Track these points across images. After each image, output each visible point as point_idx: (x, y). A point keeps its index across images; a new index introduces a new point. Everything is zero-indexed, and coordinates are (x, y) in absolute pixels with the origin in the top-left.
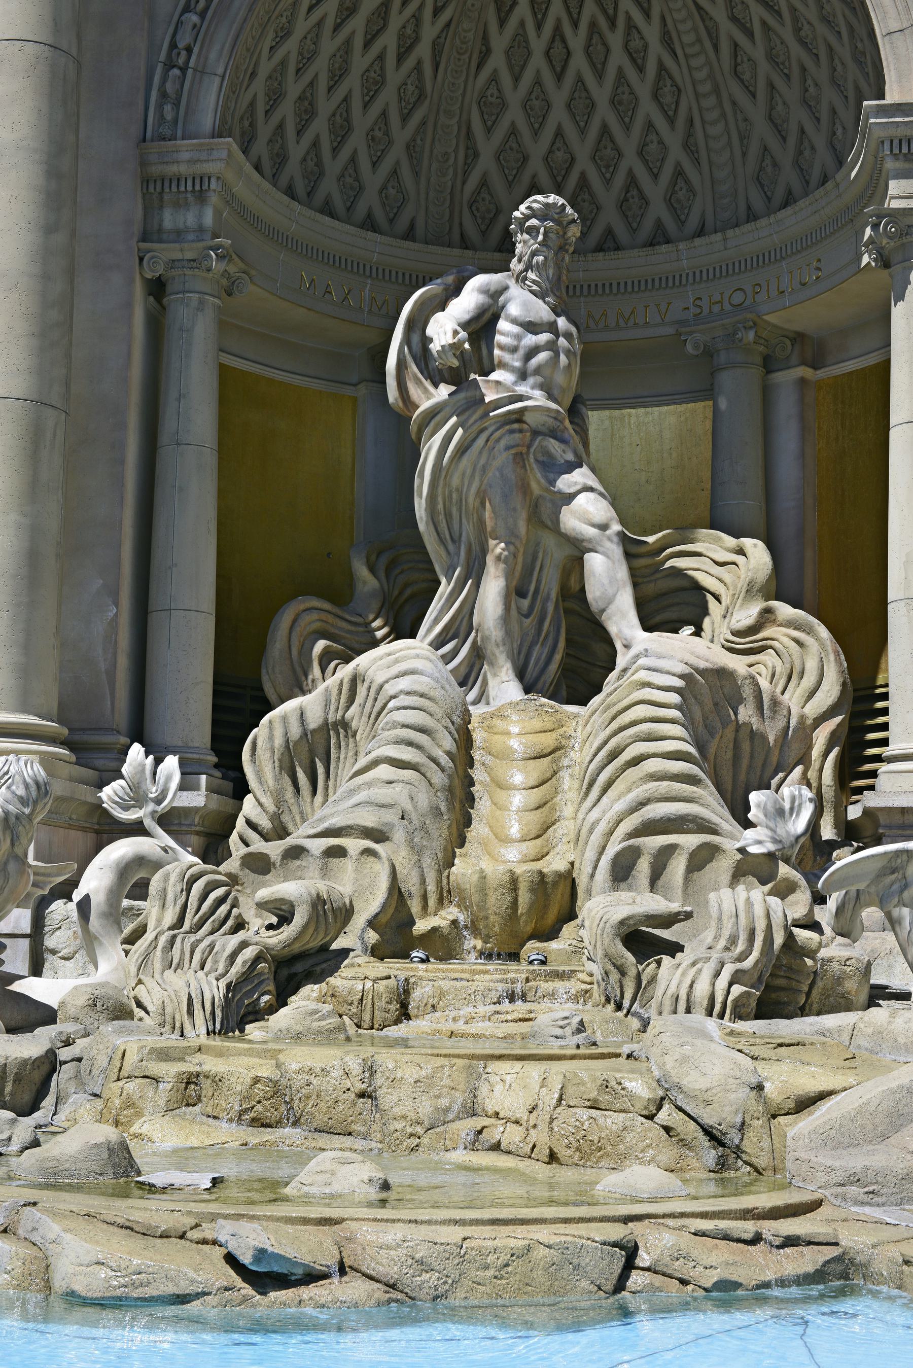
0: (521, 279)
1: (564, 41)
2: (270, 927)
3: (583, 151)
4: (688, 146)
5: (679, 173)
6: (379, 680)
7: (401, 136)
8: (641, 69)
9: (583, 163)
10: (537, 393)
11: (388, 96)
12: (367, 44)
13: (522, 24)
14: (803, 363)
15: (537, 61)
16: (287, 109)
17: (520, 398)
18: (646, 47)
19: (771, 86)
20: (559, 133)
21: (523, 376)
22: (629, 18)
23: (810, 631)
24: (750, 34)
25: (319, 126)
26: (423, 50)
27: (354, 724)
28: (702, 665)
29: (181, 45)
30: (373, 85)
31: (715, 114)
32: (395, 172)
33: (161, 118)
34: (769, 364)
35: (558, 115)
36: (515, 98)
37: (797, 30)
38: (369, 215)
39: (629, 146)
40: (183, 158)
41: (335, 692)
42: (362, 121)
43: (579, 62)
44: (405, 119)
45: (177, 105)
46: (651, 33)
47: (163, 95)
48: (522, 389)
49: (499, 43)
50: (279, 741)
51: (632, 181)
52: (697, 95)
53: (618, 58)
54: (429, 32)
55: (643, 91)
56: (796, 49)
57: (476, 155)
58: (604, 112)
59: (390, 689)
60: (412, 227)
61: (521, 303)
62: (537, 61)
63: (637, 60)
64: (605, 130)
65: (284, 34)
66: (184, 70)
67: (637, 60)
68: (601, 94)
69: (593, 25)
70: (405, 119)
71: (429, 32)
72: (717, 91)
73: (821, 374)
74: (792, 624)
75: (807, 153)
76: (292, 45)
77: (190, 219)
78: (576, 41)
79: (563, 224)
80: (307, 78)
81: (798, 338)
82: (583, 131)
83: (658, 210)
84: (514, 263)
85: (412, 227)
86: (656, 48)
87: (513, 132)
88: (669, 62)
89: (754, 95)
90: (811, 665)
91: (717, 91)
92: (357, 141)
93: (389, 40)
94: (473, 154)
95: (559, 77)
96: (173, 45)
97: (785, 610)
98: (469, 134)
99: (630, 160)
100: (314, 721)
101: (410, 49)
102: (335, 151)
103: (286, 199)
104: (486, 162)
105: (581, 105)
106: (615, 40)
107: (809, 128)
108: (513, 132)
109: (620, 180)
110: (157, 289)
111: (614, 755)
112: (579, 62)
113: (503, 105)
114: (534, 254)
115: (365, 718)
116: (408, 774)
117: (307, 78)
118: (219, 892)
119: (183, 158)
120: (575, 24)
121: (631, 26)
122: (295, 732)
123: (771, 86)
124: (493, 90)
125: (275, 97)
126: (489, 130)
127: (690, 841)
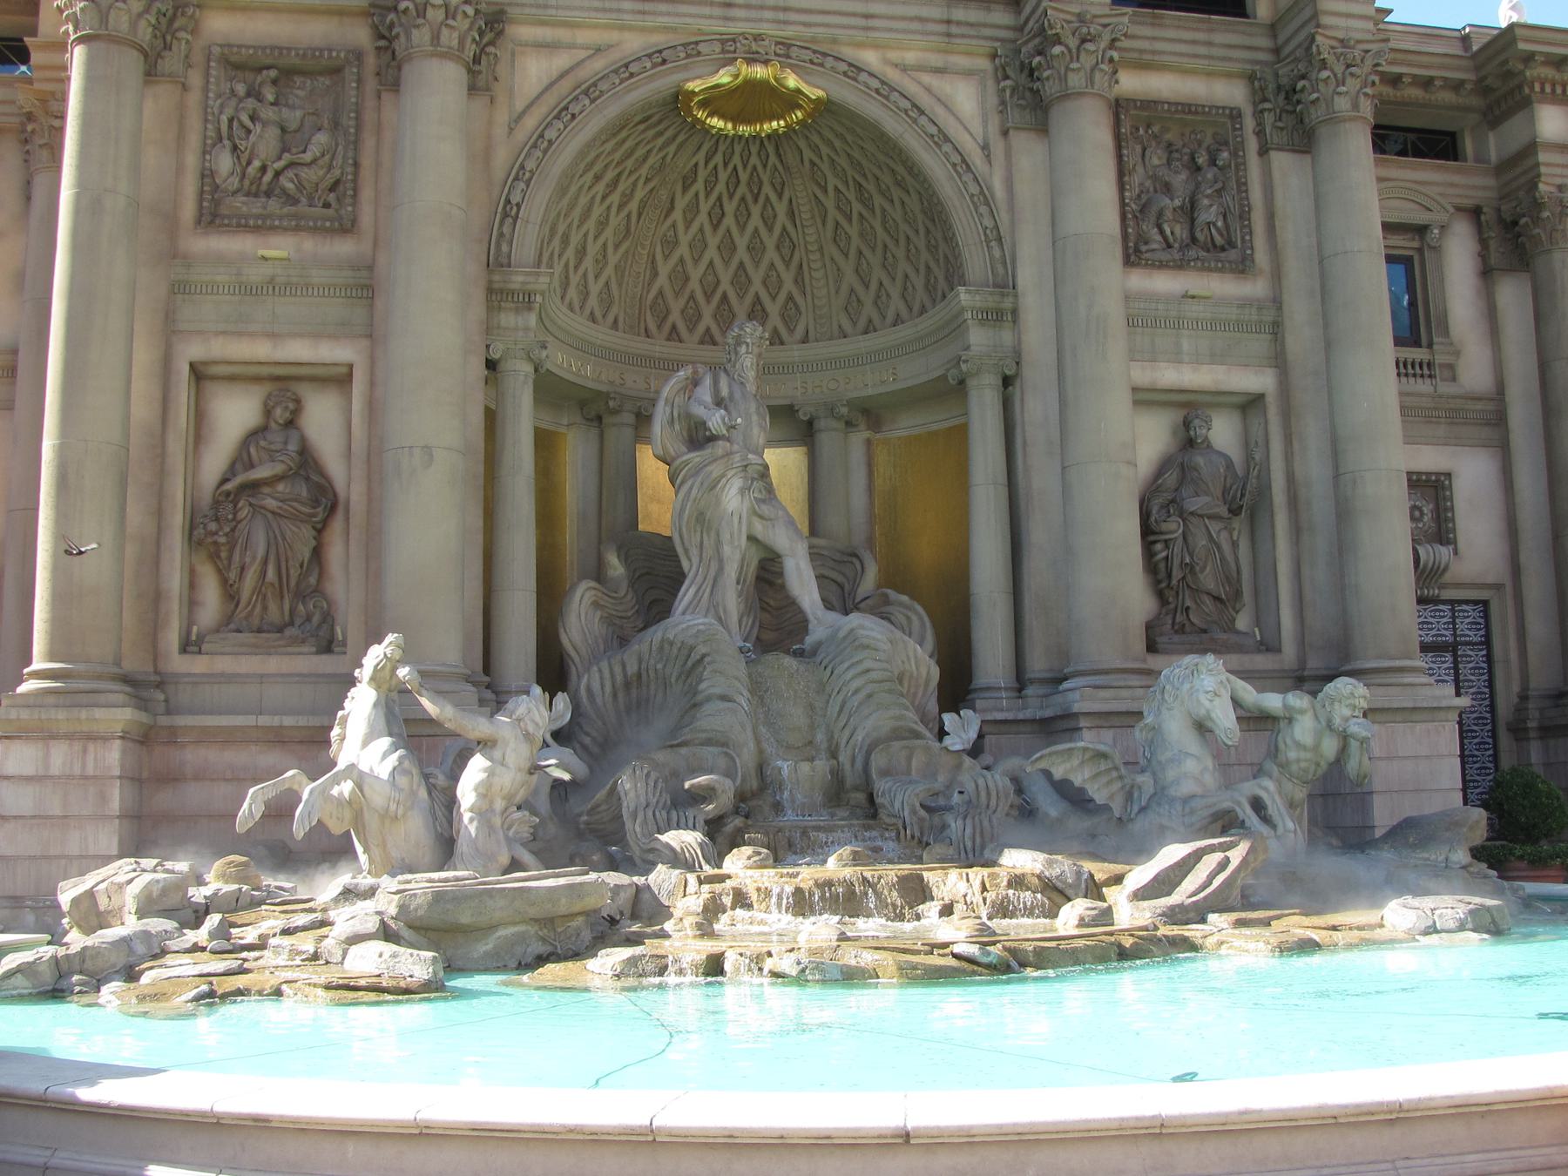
3: (725, 277)
4: (799, 281)
5: (790, 298)
7: (613, 259)
8: (770, 229)
9: (725, 286)
11: (608, 233)
15: (703, 218)
18: (775, 216)
20: (711, 263)
22: (767, 198)
26: (633, 206)
29: (514, 202)
30: (603, 224)
31: (819, 264)
35: (711, 253)
36: (684, 239)
37: (884, 222)
39: (757, 277)
40: (517, 281)
42: (593, 249)
47: (501, 235)
49: (681, 204)
53: (755, 221)
54: (640, 194)
55: (770, 243)
58: (742, 254)
60: (616, 321)
62: (703, 218)
64: (741, 265)
68: (741, 242)
69: (743, 199)
71: (640, 194)
72: (821, 249)
73: (878, 436)
74: (901, 604)
75: (884, 298)
78: (730, 208)
85: (616, 321)
86: (782, 217)
88: (790, 228)
91: (821, 249)
92: (588, 263)
94: (655, 274)
95: (715, 227)
96: (508, 201)
99: (757, 286)
101: (626, 204)
104: (662, 280)
106: (756, 210)
107: (886, 282)
108: (682, 260)
110: (491, 365)
112: (729, 221)
113: (676, 243)
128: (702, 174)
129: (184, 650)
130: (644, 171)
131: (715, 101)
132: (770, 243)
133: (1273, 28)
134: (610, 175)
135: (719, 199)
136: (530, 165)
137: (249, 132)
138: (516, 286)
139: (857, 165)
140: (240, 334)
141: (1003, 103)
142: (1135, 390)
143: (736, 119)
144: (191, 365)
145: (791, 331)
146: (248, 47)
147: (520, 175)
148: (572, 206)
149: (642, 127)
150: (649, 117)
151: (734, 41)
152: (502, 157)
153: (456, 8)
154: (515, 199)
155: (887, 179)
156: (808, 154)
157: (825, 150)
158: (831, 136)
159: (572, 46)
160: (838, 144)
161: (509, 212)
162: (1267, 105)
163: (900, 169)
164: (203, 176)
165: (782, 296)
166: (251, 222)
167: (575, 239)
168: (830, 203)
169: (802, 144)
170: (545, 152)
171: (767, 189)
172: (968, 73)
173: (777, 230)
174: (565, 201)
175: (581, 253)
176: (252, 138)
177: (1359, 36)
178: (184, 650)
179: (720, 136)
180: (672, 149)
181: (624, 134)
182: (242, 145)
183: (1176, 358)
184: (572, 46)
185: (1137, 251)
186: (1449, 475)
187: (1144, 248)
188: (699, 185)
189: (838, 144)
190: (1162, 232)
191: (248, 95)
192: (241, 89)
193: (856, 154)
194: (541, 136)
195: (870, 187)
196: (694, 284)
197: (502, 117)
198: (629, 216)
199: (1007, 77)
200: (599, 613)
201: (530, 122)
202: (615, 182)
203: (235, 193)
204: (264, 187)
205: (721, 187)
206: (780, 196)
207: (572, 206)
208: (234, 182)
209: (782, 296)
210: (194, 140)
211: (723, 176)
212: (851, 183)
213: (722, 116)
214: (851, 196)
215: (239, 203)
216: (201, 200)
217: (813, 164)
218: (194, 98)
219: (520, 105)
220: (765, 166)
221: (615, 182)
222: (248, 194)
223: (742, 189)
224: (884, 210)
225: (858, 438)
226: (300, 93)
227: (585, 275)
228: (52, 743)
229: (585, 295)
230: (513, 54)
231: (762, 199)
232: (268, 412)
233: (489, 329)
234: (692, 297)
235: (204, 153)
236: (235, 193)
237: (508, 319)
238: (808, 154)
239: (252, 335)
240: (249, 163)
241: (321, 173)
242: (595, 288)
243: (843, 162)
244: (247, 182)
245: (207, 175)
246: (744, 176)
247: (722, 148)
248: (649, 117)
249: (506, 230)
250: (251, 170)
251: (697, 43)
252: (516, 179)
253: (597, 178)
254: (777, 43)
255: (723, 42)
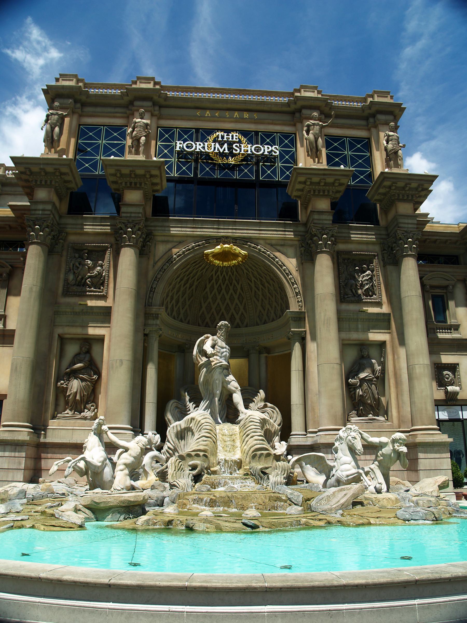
0: (219, 338)
1: (221, 287)
2: (190, 470)
4: (245, 308)
5: (242, 314)
6: (199, 419)
8: (236, 293)
9: (223, 310)
10: (224, 361)
12: (184, 285)
13: (213, 283)
14: (266, 353)
15: (215, 290)
17: (221, 362)
18: (237, 289)
19: (262, 300)
20: (218, 304)
21: (221, 357)
22: (234, 284)
23: (274, 409)
24: (259, 290)
25: (174, 301)
26: (194, 287)
27: (192, 428)
28: (262, 418)
29: (153, 287)
30: (184, 294)
32: (186, 310)
33: (149, 301)
34: (260, 353)
35: (218, 300)
37: (269, 291)
38: (181, 319)
40: (154, 310)
41: (187, 421)
42: (181, 300)
43: (224, 291)
44: (189, 300)
45: (152, 299)
46: (239, 287)
47: (149, 297)
48: (221, 360)
49: (208, 286)
50: (175, 431)
51: (233, 315)
52: (247, 299)
53: (231, 291)
54: (196, 283)
55: (236, 297)
56: (268, 294)
57: (202, 307)
58: (228, 301)
59: (203, 421)
60: (189, 321)
61: (221, 343)
62: (215, 290)
63: (235, 291)
64: (228, 304)
65: (171, 284)
66: (154, 292)
67: (235, 291)
68: (227, 297)
69: (227, 284)
70: (189, 300)
71: (196, 283)
73: (269, 355)
74: (270, 407)
76: (171, 286)
77: (154, 322)
78: (223, 287)
79: (228, 327)
81: (265, 348)
82: (223, 304)
84: (218, 334)
85: (189, 321)
87: (209, 303)
88: (241, 292)
89: (258, 301)
90: (275, 416)
92: (180, 304)
93: (188, 285)
94: (201, 307)
95: (219, 293)
96: (152, 287)
97: (269, 405)
98: (201, 303)
100: (183, 427)
102: (176, 306)
103: (173, 320)
104: (204, 309)
106: (231, 288)
107: (270, 309)
108: (209, 303)
109: (230, 314)
110: (146, 335)
111: (248, 435)
112: (224, 291)
114: (222, 333)
115: (195, 427)
116: (209, 439)
118: (181, 463)
119: (154, 310)
120: (224, 284)
121: (235, 285)
122: (179, 429)
123: (262, 300)
126: (205, 302)
127: (265, 452)
128: (214, 277)
130: (196, 277)
131: (216, 256)
132: (236, 297)
133: (386, 228)
134: (185, 278)
135: (220, 285)
136: (159, 276)
137: (78, 268)
138: (153, 312)
139: (260, 275)
140: (73, 326)
141: (301, 254)
142: (343, 340)
143: (223, 261)
144: (59, 335)
145: (243, 324)
146: (80, 244)
147: (156, 279)
148: (173, 288)
149: (194, 264)
150: (196, 262)
151: (220, 238)
152: (151, 274)
153: (136, 232)
154: (154, 286)
155: (268, 278)
156: (245, 271)
157: (250, 270)
158: (251, 265)
159: (172, 242)
160: (254, 268)
161: (152, 290)
162: (385, 252)
163: (271, 275)
164: (65, 281)
165: (240, 313)
166: (78, 294)
167: (175, 297)
168: (253, 285)
169: (243, 268)
170: (163, 272)
171: (234, 281)
172: (291, 246)
173: (238, 293)
174: (171, 286)
175: (177, 302)
176: (79, 270)
177: (412, 230)
179: (218, 267)
180: (204, 270)
181: (189, 266)
182: (76, 271)
183: (357, 330)
184: (172, 242)
185: (344, 298)
186: (458, 364)
187: (346, 297)
188: (214, 281)
189: (254, 268)
190: (352, 292)
191: (79, 257)
192: (77, 255)
193: (259, 271)
194: (162, 268)
195: (264, 280)
196: (213, 310)
197: (151, 262)
198: (192, 290)
199: (302, 247)
200: (177, 410)
201: (160, 264)
202: (188, 280)
203: (74, 285)
204: (82, 284)
205: (220, 281)
206: (238, 284)
207: (173, 288)
208: (74, 282)
209: (240, 313)
210: (63, 270)
211: (221, 278)
212: (258, 279)
213: (219, 260)
214: (259, 283)
215: (75, 288)
216: (64, 287)
217: (247, 274)
218: (64, 258)
219: (157, 259)
220: (233, 275)
221: (188, 280)
222: (78, 286)
223: (227, 282)
224: (268, 287)
225: (263, 356)
226: (94, 256)
227: (179, 308)
228: (6, 446)
229: (179, 314)
230: (155, 244)
231: (233, 284)
232: (81, 349)
233: (145, 325)
234: (213, 314)
235: (66, 274)
236: (74, 285)
237: (151, 322)
238: (245, 271)
239: (76, 326)
240: (78, 277)
241: (98, 279)
242: (182, 312)
243: (255, 273)
244: (77, 282)
245: (66, 280)
246: (227, 278)
247: (219, 270)
248: (196, 262)
249: (151, 295)
250: (79, 279)
251: (209, 240)
252: (155, 280)
253: (182, 280)
254: (233, 239)
255: (217, 239)
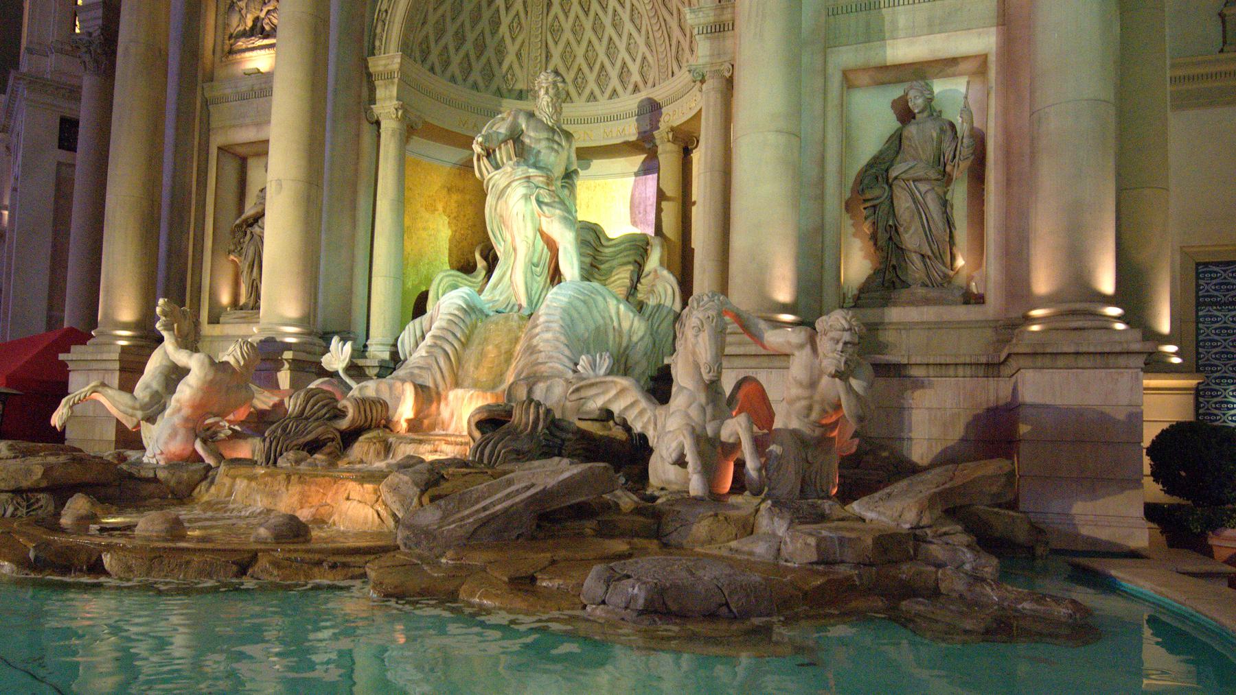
4: (648, 45)
16: (448, 38)
80: (459, 22)
83: (636, 77)
94: (548, 56)
105: (598, 28)
117: (459, 22)
124: (556, 23)
125: (440, 33)
129: (209, 323)
178: (209, 323)
